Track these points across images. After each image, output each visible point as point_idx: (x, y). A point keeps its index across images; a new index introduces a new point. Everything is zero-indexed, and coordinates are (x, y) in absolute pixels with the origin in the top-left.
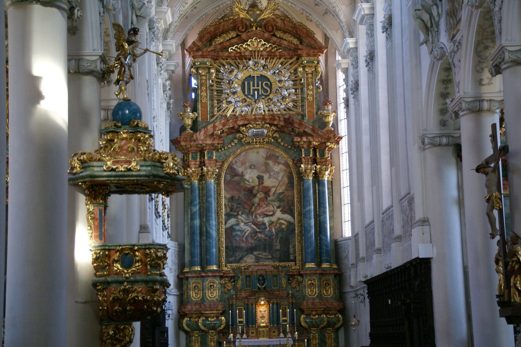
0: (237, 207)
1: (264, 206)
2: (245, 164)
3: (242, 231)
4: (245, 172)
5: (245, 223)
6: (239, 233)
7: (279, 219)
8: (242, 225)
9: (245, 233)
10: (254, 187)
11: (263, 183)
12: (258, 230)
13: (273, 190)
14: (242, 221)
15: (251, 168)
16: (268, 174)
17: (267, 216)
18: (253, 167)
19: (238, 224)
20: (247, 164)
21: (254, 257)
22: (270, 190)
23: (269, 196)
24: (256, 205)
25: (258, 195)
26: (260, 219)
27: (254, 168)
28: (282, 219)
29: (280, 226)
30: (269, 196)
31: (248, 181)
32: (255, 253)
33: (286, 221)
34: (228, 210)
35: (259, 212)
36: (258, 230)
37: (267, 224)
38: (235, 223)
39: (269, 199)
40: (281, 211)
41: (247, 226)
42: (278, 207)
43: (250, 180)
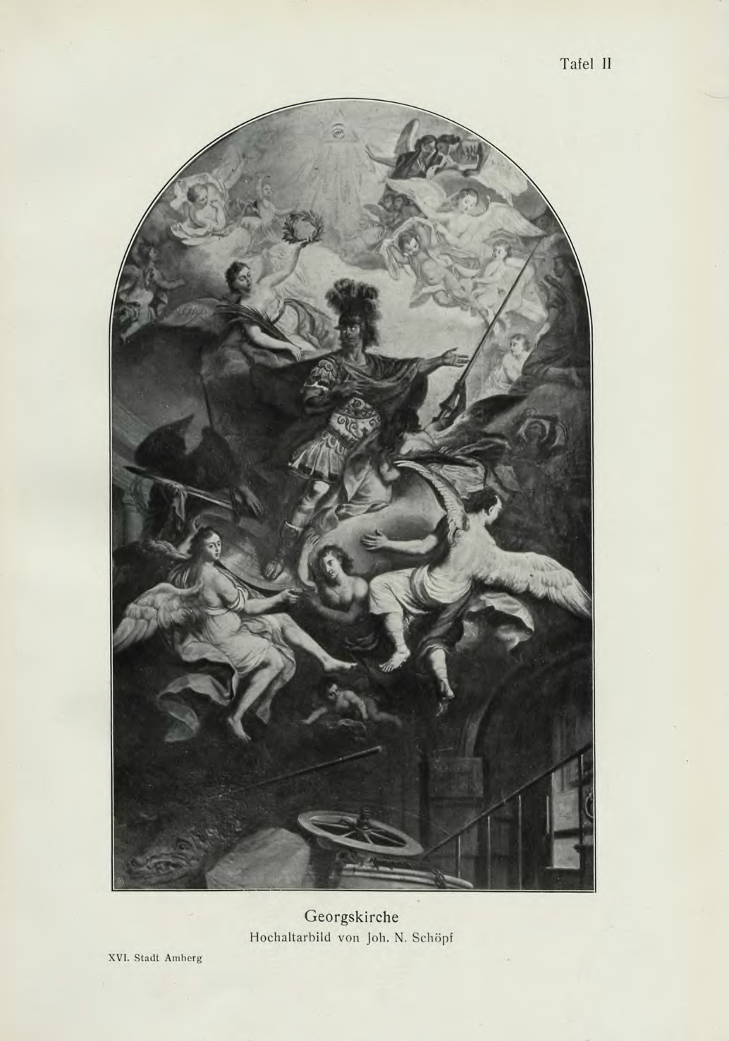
0: (194, 506)
1: (378, 492)
2: (254, 207)
3: (221, 671)
4: (253, 267)
5: (242, 614)
6: (202, 684)
7: (479, 586)
8: (224, 624)
9: (246, 683)
10: (305, 369)
11: (370, 336)
12: (331, 663)
13: (440, 384)
14: (225, 604)
15: (291, 236)
16: (407, 278)
17: (396, 561)
18: (305, 229)
19: (195, 625)
20: (268, 213)
21: (304, 851)
22: (419, 387)
23: (415, 428)
24: (322, 487)
25: (338, 422)
26: (350, 587)
27: (315, 238)
28: (499, 587)
29: (489, 639)
30: (415, 428)
31: (269, 328)
32: (305, 822)
33: (527, 597)
34: (137, 522)
35: (344, 533)
36: (331, 663)
37: (397, 627)
38: (178, 615)
39: (412, 443)
40: (493, 528)
41: (262, 634)
42: (476, 504)
43: (288, 322)
